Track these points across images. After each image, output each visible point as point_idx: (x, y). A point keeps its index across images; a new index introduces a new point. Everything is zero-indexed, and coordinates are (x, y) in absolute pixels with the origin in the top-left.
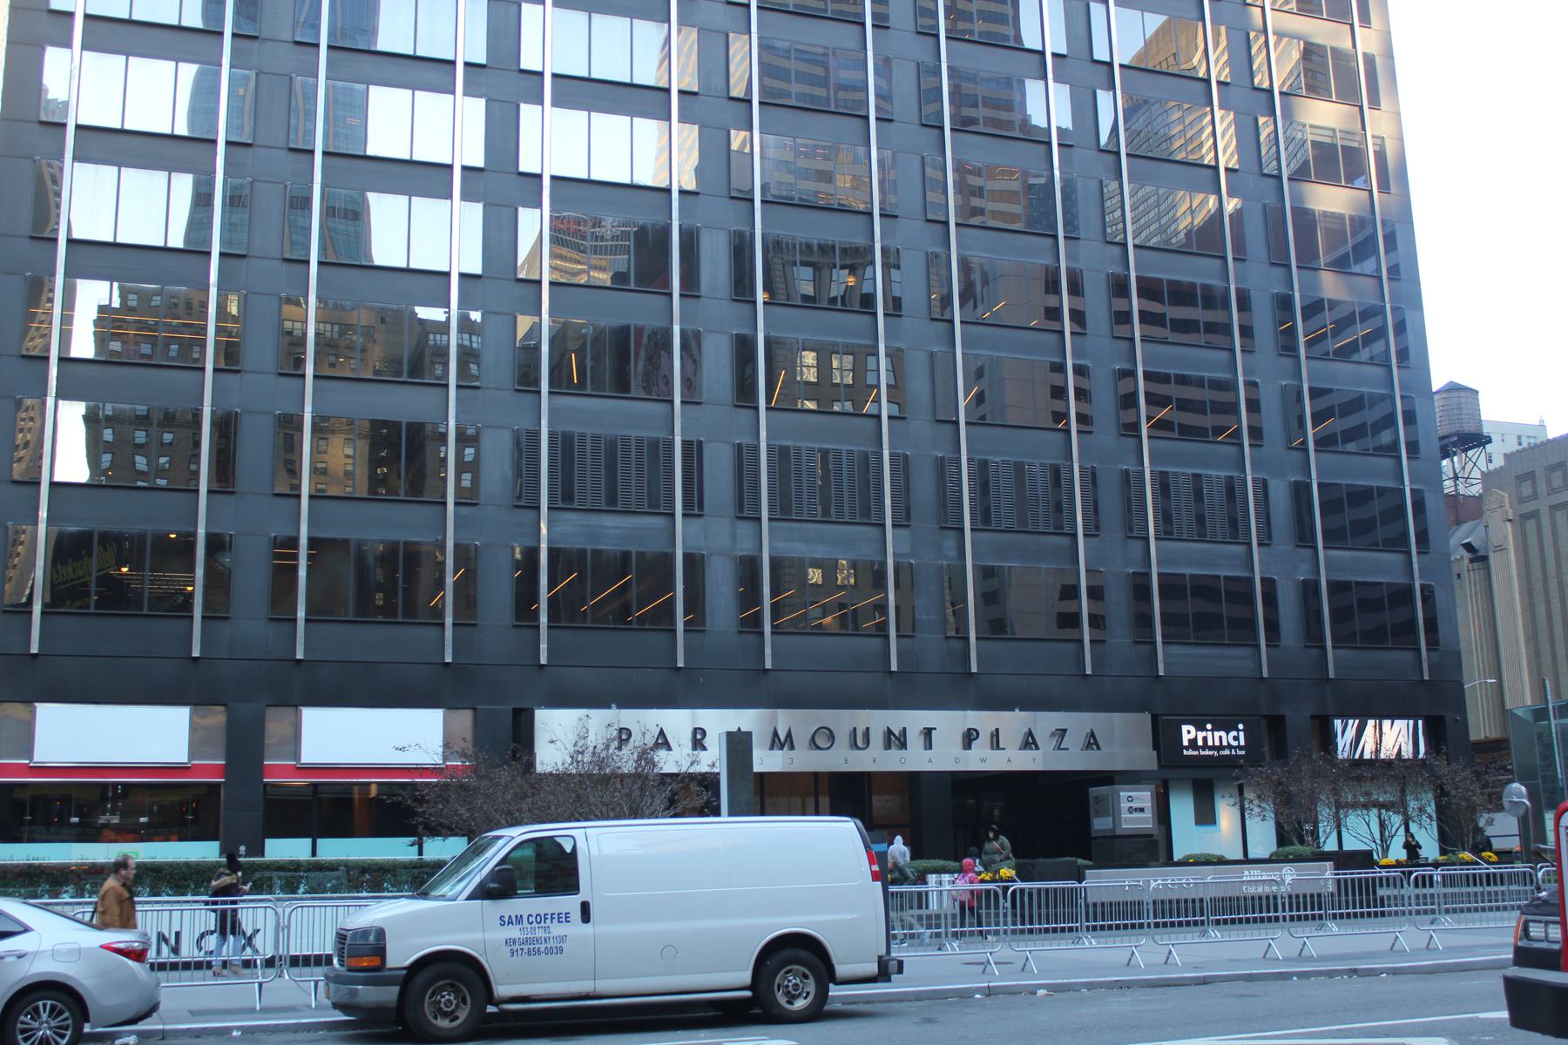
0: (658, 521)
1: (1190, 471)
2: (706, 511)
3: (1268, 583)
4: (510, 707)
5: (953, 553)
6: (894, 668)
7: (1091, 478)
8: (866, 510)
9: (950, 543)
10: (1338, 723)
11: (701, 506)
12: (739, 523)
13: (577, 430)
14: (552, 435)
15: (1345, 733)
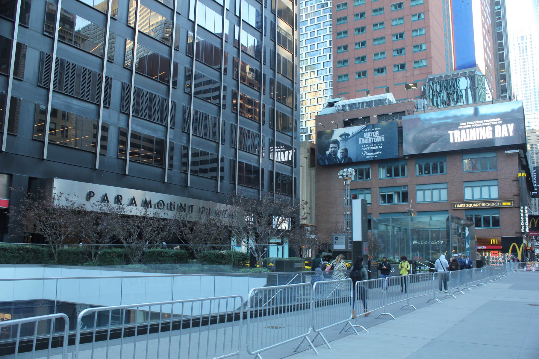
0: (93, 107)
1: (248, 129)
2: (111, 107)
3: (263, 170)
4: (28, 176)
5: (185, 142)
6: (166, 181)
7: (224, 123)
8: (162, 120)
9: (184, 138)
10: (274, 217)
11: (109, 104)
12: (121, 115)
13: (67, 60)
14: (57, 59)
15: (276, 219)
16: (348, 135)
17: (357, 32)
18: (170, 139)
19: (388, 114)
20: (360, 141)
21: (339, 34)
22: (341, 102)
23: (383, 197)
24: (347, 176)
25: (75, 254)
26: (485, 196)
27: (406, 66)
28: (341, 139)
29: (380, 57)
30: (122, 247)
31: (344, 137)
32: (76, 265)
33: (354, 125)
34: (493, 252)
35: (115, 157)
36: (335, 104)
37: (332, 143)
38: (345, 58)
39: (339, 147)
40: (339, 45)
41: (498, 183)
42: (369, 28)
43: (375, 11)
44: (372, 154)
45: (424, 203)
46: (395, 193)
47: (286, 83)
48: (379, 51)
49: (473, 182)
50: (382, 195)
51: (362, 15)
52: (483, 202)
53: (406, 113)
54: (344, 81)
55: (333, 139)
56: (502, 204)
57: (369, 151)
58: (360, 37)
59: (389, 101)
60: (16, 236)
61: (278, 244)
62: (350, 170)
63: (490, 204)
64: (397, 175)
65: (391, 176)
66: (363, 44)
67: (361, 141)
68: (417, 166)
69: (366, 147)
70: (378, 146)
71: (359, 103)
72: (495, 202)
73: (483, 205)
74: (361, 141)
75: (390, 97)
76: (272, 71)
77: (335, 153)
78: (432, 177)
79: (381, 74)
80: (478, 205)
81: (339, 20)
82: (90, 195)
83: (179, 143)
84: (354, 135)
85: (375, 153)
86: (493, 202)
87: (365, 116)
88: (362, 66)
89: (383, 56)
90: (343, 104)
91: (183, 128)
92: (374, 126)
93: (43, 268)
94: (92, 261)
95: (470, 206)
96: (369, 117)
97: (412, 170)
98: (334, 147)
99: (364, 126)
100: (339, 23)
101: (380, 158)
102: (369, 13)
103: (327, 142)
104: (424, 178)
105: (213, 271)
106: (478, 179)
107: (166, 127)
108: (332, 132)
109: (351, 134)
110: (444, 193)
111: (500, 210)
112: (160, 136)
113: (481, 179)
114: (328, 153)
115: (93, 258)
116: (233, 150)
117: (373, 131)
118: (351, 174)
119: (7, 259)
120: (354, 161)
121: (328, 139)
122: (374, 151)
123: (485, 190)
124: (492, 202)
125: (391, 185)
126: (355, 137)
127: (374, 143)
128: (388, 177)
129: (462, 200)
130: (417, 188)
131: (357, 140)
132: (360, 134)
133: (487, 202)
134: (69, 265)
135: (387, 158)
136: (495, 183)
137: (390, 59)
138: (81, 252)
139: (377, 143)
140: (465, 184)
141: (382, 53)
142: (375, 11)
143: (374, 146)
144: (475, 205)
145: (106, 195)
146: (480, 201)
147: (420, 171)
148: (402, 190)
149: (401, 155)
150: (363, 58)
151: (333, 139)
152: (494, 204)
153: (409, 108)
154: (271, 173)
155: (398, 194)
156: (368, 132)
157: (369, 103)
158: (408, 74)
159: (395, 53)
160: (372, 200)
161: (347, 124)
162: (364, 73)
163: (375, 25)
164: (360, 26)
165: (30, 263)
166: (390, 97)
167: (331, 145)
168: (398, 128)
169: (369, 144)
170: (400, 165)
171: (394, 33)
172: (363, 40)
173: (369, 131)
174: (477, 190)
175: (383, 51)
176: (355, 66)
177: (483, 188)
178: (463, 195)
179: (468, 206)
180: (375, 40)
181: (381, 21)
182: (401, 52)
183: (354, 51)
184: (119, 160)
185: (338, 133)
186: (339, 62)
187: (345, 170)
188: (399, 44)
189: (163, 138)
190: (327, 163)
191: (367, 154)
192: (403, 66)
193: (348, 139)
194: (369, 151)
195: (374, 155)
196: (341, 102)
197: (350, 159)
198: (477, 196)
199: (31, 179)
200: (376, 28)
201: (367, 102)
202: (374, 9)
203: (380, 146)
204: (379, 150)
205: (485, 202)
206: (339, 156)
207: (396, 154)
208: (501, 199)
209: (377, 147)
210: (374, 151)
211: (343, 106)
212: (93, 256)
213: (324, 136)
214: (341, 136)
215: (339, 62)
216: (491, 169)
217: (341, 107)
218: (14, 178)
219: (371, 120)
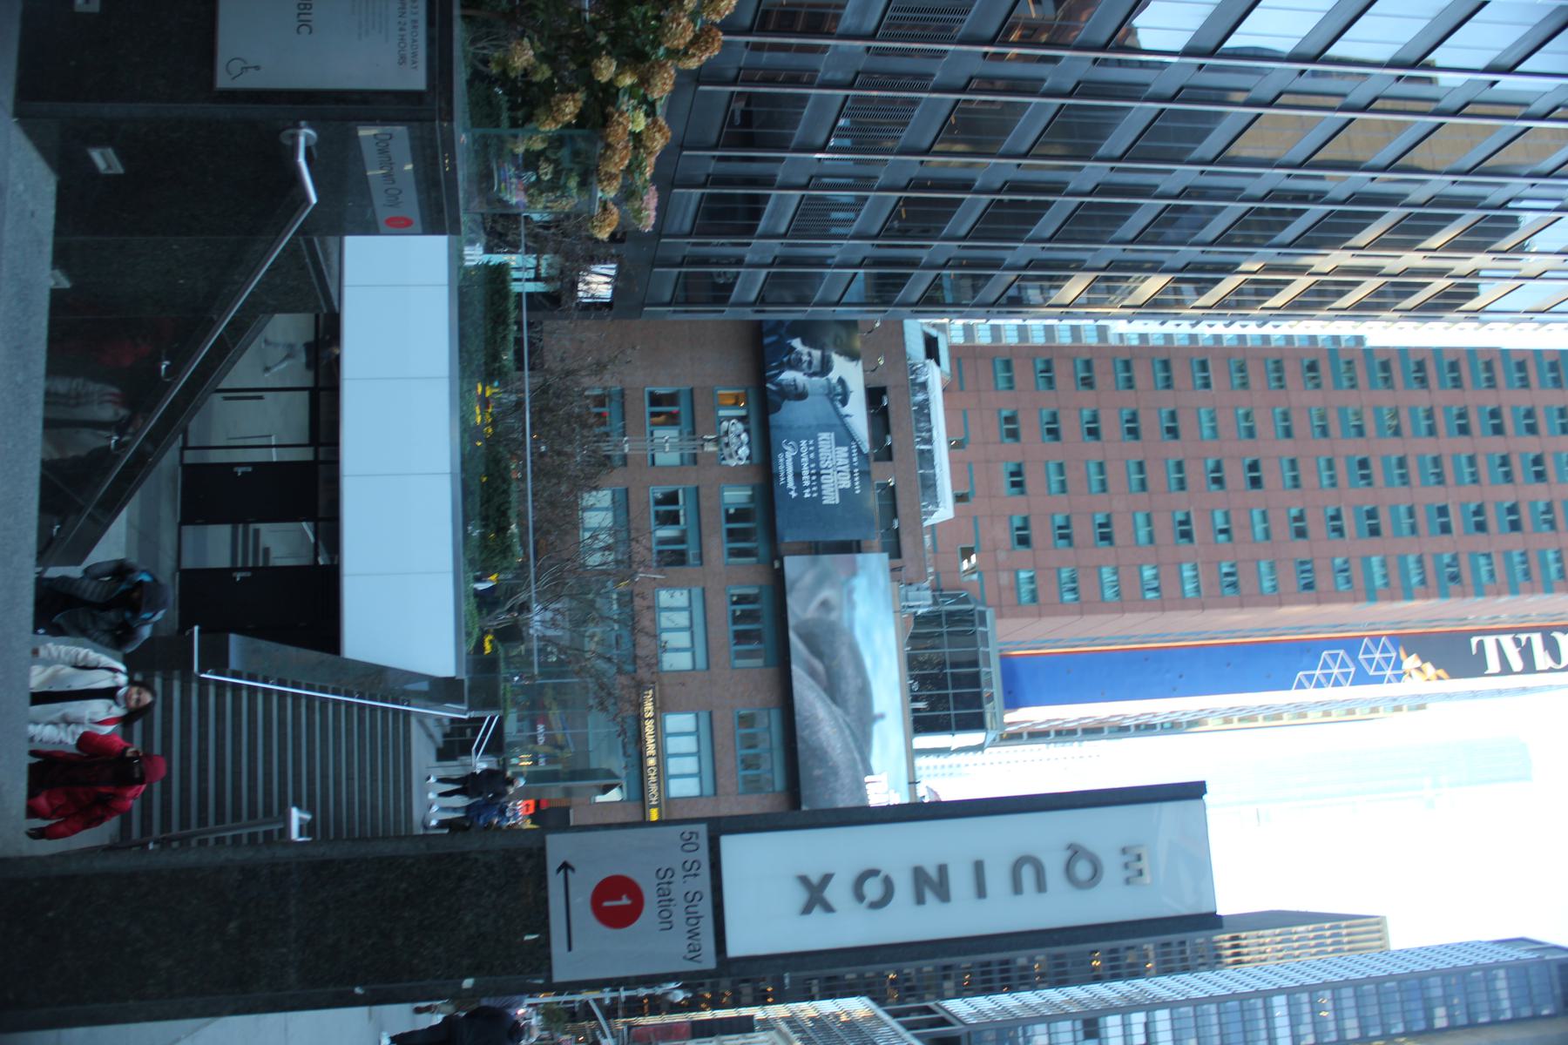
5: (829, 76)
9: (839, 76)
15: (610, 269)
16: (844, 402)
17: (1126, 414)
19: (895, 515)
20: (823, 436)
21: (1127, 366)
22: (935, 376)
23: (671, 498)
24: (727, 445)
26: (674, 766)
27: (1022, 550)
28: (834, 381)
29: (1055, 479)
31: (839, 389)
33: (872, 419)
36: (932, 363)
38: (1060, 381)
40: (1096, 363)
42: (1134, 451)
43: (1179, 466)
44: (790, 470)
45: (653, 608)
47: (991, 292)
48: (1071, 476)
51: (1173, 432)
53: (897, 562)
54: (995, 378)
57: (797, 460)
58: (1112, 426)
59: (932, 513)
61: (537, 268)
63: (653, 779)
65: (730, 518)
66: (1093, 433)
67: (826, 439)
71: (930, 430)
73: (652, 762)
74: (826, 439)
75: (945, 511)
76: (1024, 262)
77: (795, 365)
78: (725, 630)
79: (1006, 481)
80: (651, 749)
81: (1166, 365)
83: (825, 66)
84: (842, 417)
85: (790, 479)
87: (895, 449)
88: (1031, 428)
89: (1055, 487)
90: (930, 383)
91: (868, 72)
92: (865, 474)
95: (649, 727)
96: (890, 458)
97: (746, 578)
98: (810, 363)
99: (866, 448)
100: (1158, 366)
101: (777, 492)
102: (1175, 450)
104: (722, 610)
106: (718, 748)
107: (872, 37)
108: (853, 356)
110: (682, 661)
111: (639, 803)
112: (848, 21)
113: (718, 756)
114: (797, 343)
115: (480, 45)
116: (803, 180)
117: (852, 473)
120: (774, 419)
121: (835, 345)
122: (798, 476)
123: (690, 765)
124: (658, 782)
125: (704, 520)
126: (837, 421)
127: (819, 475)
129: (662, 708)
130: (697, 591)
132: (845, 436)
136: (708, 790)
137: (1044, 505)
139: (819, 484)
140: (704, 716)
141: (1063, 484)
142: (1179, 466)
146: (662, 755)
147: (742, 599)
148: (692, 552)
150: (1054, 433)
152: (654, 788)
153: (910, 570)
154: (739, 262)
155: (681, 540)
156: (850, 457)
157: (927, 458)
158: (1002, 556)
159: (1059, 520)
160: (664, 468)
161: (875, 396)
162: (1013, 434)
163: (1141, 467)
164: (1144, 423)
166: (945, 511)
167: (817, 354)
168: (858, 542)
169: (816, 460)
170: (758, 544)
171: (1115, 520)
172: (1104, 433)
173: (851, 463)
174: (688, 744)
175: (1069, 487)
176: (1033, 410)
178: (679, 709)
180: (1101, 466)
181: (1150, 485)
182: (1062, 537)
183: (1075, 406)
185: (850, 372)
186: (1048, 362)
187: (744, 437)
188: (1084, 531)
189: (841, 28)
190: (767, 341)
192: (1024, 541)
193: (832, 401)
194: (797, 460)
196: (935, 376)
197: (778, 408)
198: (673, 745)
200: (1133, 468)
201: (930, 452)
202: (1186, 466)
204: (800, 488)
206: (788, 376)
207: (788, 536)
208: (667, 802)
210: (798, 476)
211: (924, 386)
214: (841, 381)
215: (1048, 362)
217: (921, 379)
219: (881, 464)
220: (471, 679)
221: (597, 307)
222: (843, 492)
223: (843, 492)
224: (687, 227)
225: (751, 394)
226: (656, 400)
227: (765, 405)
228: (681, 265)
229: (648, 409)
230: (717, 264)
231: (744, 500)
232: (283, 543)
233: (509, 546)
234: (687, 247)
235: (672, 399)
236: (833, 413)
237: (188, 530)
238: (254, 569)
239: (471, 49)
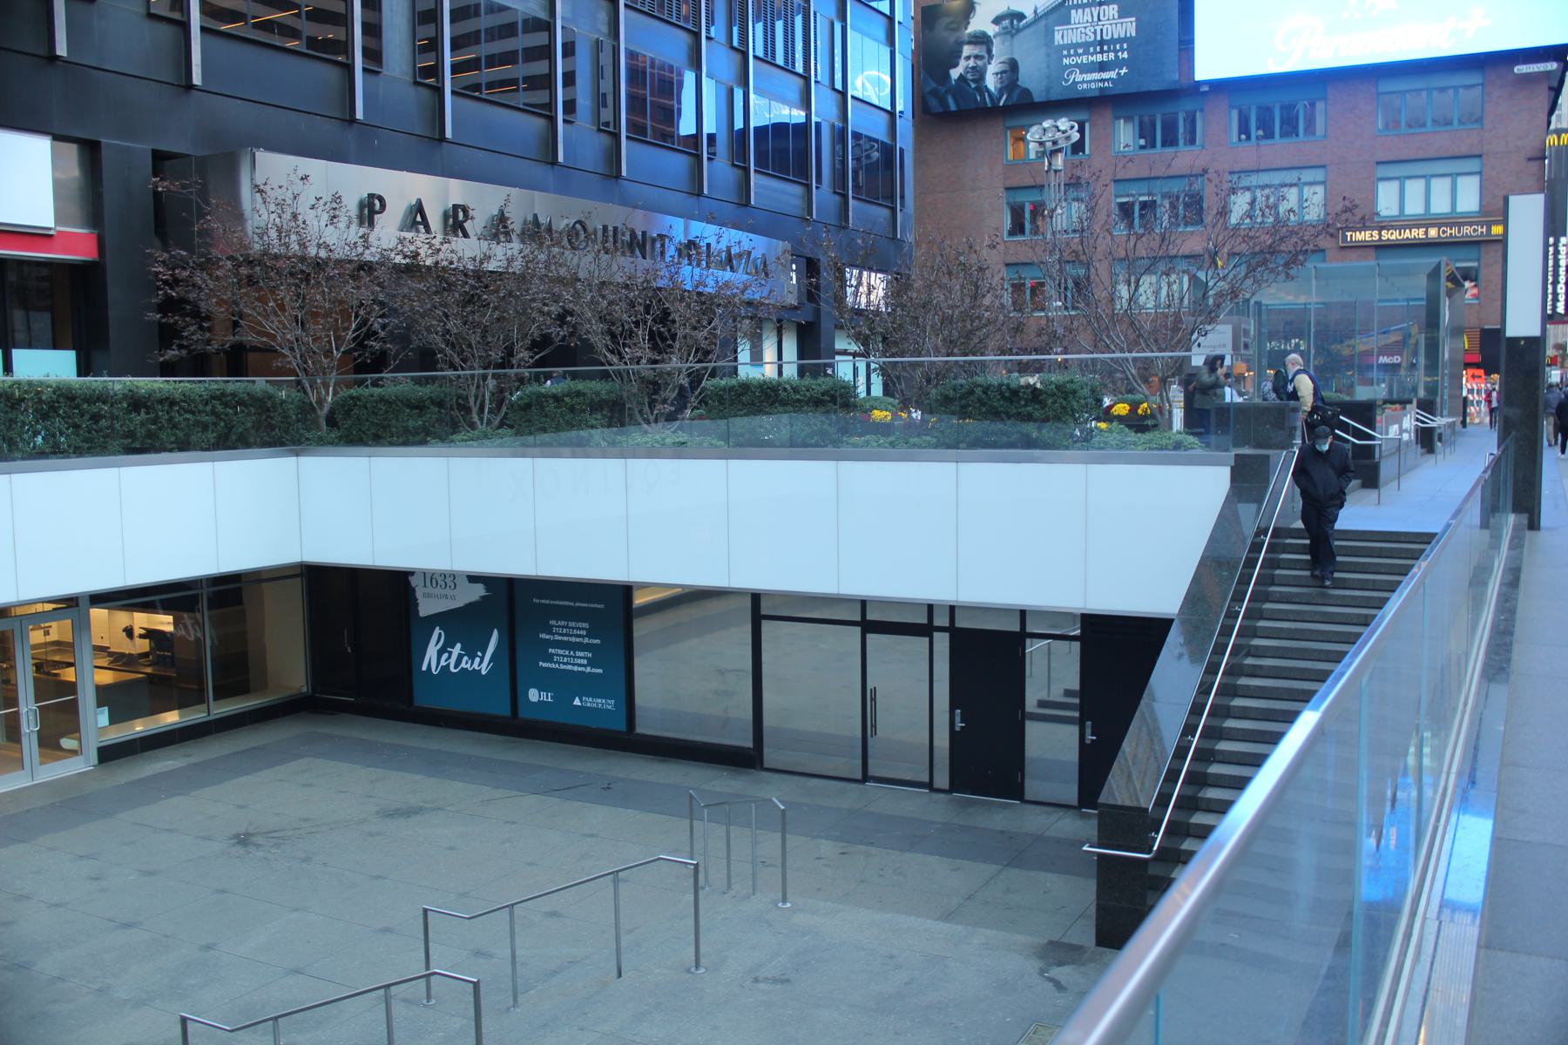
4: (148, 147)
5: (604, 29)
9: (603, 16)
16: (1021, 16)
18: (563, 19)
20: (1058, 38)
24: (1055, 143)
25: (413, 407)
26: (1440, 206)
28: (997, 29)
30: (605, 376)
31: (1006, 23)
32: (423, 443)
34: (1471, 372)
35: (409, 78)
37: (970, 43)
39: (991, 56)
41: (1483, 165)
44: (1096, 76)
46: (1164, 196)
49: (1402, 163)
50: (1121, 205)
52: (1433, 225)
55: (971, 29)
56: (1489, 230)
57: (1085, 69)
60: (184, 352)
61: (854, 355)
62: (1063, 123)
63: (1454, 231)
64: (1170, 141)
65: (1153, 146)
67: (1062, 36)
68: (1235, 113)
69: (1076, 54)
70: (1116, 52)
72: (1471, 224)
73: (1433, 232)
74: (1062, 36)
77: (979, 74)
80: (1418, 233)
82: (371, 208)
84: (1038, 18)
85: (1106, 75)
86: (1464, 224)
93: (293, 459)
94: (472, 426)
98: (976, 57)
101: (1121, 90)
103: (952, 39)
105: (770, 444)
106: (1421, 155)
109: (1029, 15)
111: (1483, 248)
113: (1432, 154)
114: (955, 73)
115: (476, 418)
118: (1068, 138)
119: (180, 434)
121: (957, 29)
122: (1103, 67)
123: (1440, 187)
126: (1043, 22)
127: (1102, 43)
128: (1142, 147)
131: (1049, 34)
133: (1446, 225)
134: (392, 444)
135: (1144, 89)
136: (1474, 165)
138: (433, 402)
139: (1113, 41)
140: (1382, 171)
143: (1102, 52)
144: (1407, 234)
145: (419, 203)
147: (1244, 129)
149: (1184, 81)
151: (971, 29)
152: (1467, 230)
165: (248, 445)
167: (967, 50)
169: (1086, 45)
170: (1181, 110)
174: (1415, 188)
177: (1435, 182)
179: (1386, 235)
184: (421, 89)
187: (1046, 124)
189: (543, 16)
190: (953, 107)
191: (1079, 78)
193: (1019, 30)
195: (1102, 81)
197: (1027, 92)
198: (1414, 207)
199: (159, 158)
203: (1123, 51)
204: (1117, 64)
205: (1439, 226)
206: (991, 82)
207: (1173, 76)
209: (1112, 56)
210: (1103, 67)
212: (475, 410)
213: (945, 21)
214: (997, 21)
216: (1409, 126)
218: (104, 152)
220: (1236, 445)
221: (899, 287)
222: (1123, 14)
223: (1123, 14)
224: (797, 190)
225: (1010, 123)
226: (1018, 228)
227: (1021, 106)
228: (845, 197)
229: (1026, 237)
230: (844, 162)
231: (1130, 127)
232: (1053, 673)
233: (1057, 387)
234: (823, 195)
235: (1017, 213)
236: (1032, 29)
237: (1032, 788)
238: (1081, 708)
239: (481, 427)
